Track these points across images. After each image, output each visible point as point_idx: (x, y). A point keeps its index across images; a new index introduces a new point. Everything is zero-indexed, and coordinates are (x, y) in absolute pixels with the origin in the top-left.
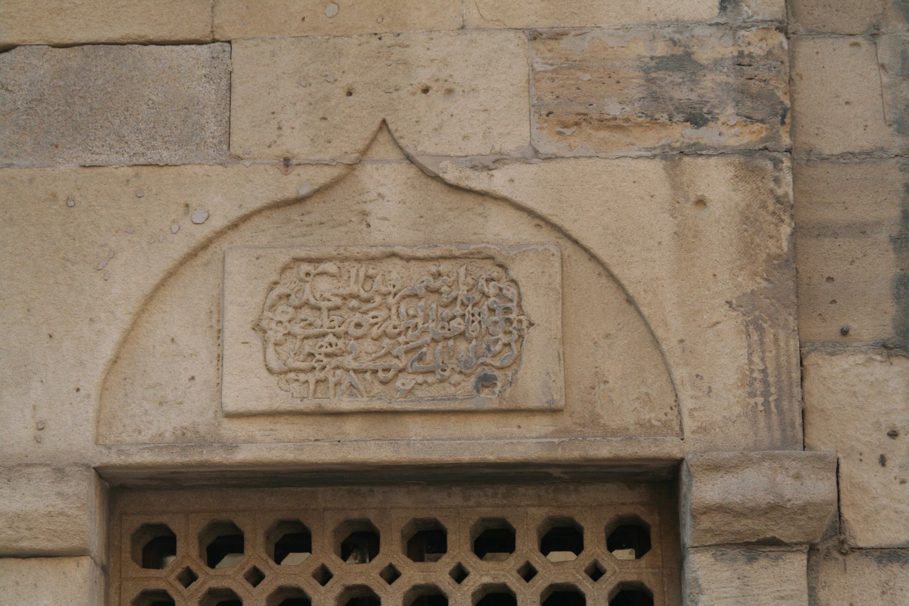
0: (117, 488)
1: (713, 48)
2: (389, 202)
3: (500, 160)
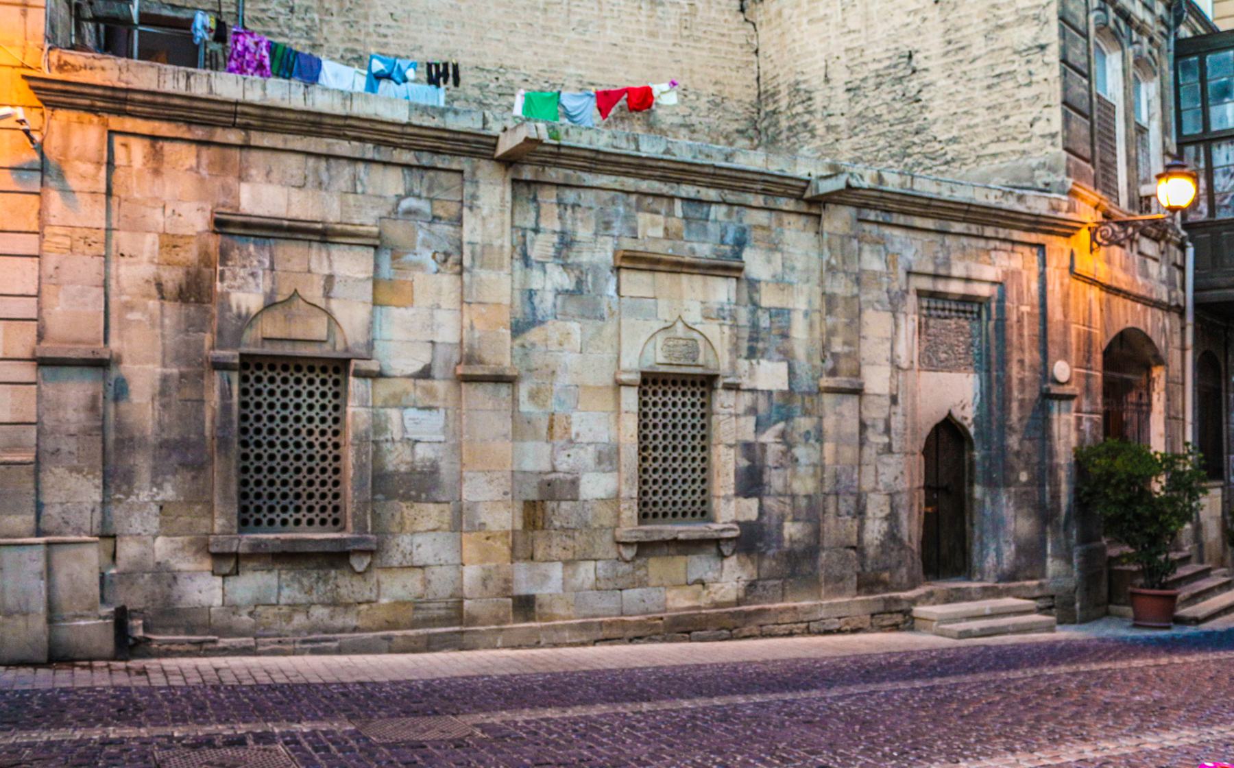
0: (643, 373)
1: (727, 308)
2: (680, 330)
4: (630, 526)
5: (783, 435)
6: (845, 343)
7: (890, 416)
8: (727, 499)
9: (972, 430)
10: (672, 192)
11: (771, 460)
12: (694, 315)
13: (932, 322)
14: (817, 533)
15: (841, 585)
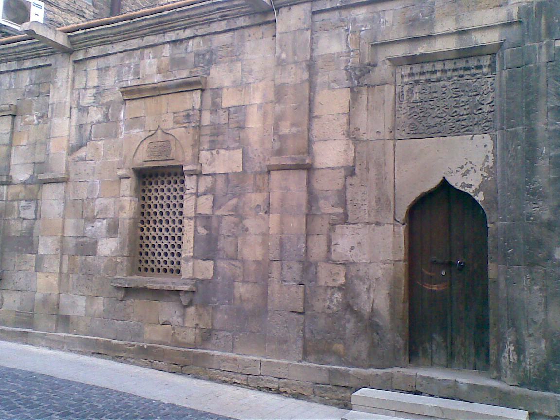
3: (169, 129)
4: (124, 278)
5: (236, 208)
6: (293, 125)
7: (345, 187)
8: (187, 260)
9: (480, 198)
10: (161, 41)
11: (224, 231)
12: (169, 124)
13: (417, 88)
14: (265, 295)
15: (285, 347)
